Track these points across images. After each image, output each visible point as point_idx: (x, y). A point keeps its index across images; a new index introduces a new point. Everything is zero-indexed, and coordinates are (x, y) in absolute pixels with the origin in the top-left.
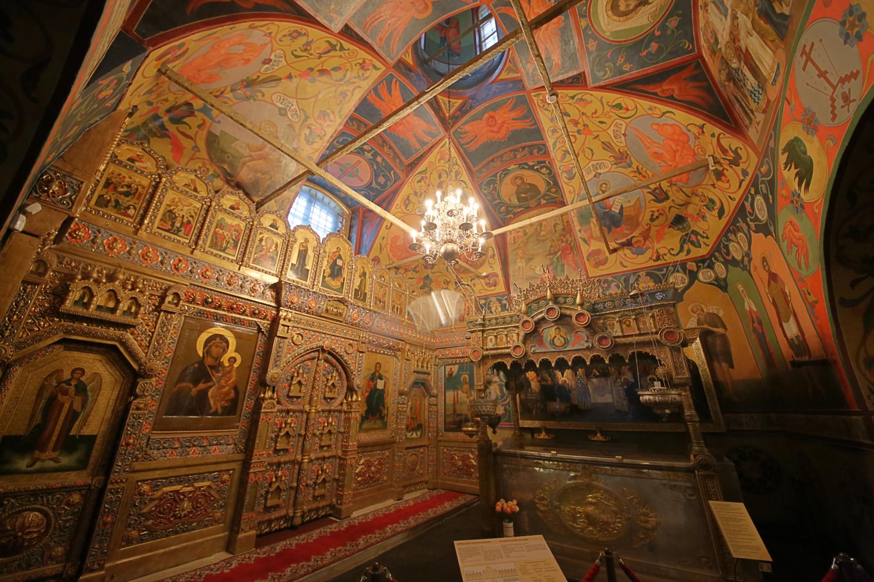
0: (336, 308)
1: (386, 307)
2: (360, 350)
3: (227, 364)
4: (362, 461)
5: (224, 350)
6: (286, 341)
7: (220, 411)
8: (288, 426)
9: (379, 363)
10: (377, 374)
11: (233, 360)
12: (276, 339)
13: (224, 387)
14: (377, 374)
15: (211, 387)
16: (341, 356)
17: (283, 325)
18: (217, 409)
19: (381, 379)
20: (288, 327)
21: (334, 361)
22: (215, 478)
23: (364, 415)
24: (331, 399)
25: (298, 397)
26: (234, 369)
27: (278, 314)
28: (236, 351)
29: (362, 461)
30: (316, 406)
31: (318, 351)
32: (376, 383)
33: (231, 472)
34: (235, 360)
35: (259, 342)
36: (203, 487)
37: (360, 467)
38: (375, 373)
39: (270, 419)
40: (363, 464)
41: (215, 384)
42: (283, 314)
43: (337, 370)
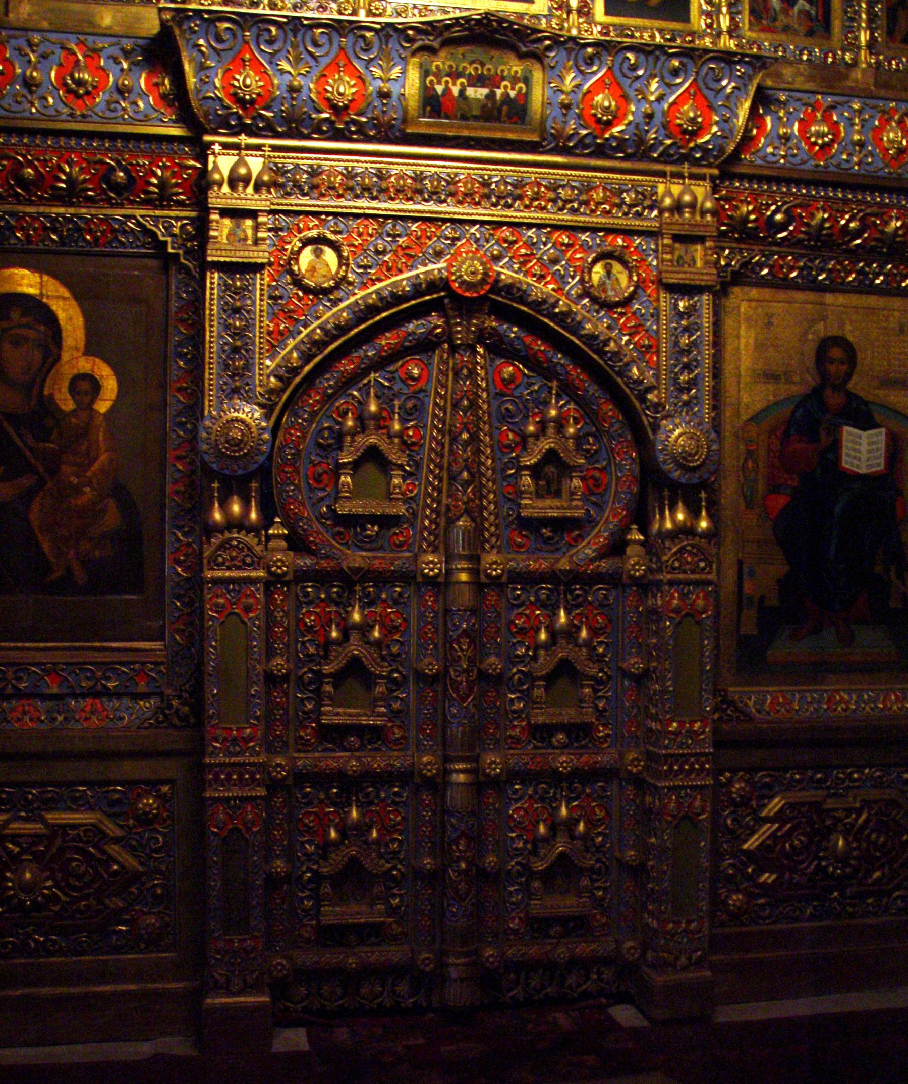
0: (478, 81)
1: (837, 25)
2: (672, 279)
3: (67, 404)
4: (776, 804)
5: (47, 354)
6: (262, 281)
7: (80, 577)
8: (354, 637)
9: (840, 341)
10: (834, 399)
11: (85, 386)
12: (214, 279)
13: (77, 490)
14: (834, 399)
15: (28, 496)
16: (563, 318)
17: (225, 213)
18: (69, 570)
19: (866, 422)
20: (253, 214)
21: (540, 346)
22: (112, 804)
23: (773, 601)
24: (561, 525)
25: (387, 522)
26: (99, 421)
27: (204, 172)
28: (91, 349)
29: (776, 804)
30: (475, 559)
31: (436, 306)
32: (836, 445)
33: (166, 789)
34: (95, 386)
35: (174, 305)
36: (74, 827)
37: (767, 829)
38: (817, 393)
39: (248, 609)
40: (779, 817)
41: (41, 483)
42: (224, 163)
43: (568, 389)
